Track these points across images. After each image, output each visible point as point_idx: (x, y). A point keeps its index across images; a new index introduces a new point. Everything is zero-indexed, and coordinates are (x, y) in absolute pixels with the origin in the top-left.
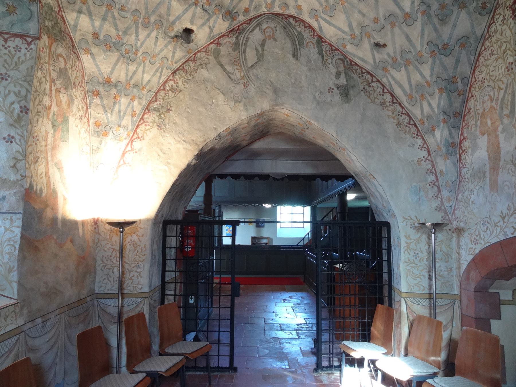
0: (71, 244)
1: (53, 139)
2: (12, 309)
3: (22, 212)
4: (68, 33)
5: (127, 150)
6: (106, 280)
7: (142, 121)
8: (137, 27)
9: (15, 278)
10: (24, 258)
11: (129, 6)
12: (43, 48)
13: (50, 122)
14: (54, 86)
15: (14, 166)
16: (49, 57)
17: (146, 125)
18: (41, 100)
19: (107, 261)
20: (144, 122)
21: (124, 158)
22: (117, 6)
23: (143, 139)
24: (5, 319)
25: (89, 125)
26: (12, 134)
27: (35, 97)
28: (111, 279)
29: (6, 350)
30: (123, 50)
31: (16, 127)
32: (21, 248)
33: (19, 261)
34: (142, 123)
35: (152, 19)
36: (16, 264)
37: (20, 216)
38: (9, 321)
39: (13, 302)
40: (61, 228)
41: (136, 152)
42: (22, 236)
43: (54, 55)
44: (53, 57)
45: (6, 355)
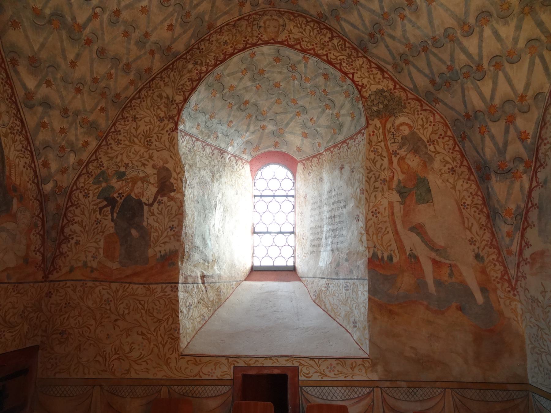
0: (460, 312)
1: (402, 206)
2: (360, 362)
3: (367, 278)
4: (413, 97)
5: (533, 186)
6: (537, 370)
7: (540, 141)
8: (460, 44)
9: (367, 336)
10: (375, 319)
11: (437, 33)
12: (373, 132)
13: (395, 192)
14: (396, 156)
15: (361, 240)
16: (384, 135)
17: (545, 145)
18: (377, 177)
19: (535, 341)
20: (543, 140)
21: (532, 199)
22: (429, 42)
23: (547, 165)
24: (351, 368)
25: (472, 173)
26: (358, 214)
27: (369, 177)
28: (541, 369)
29: (356, 396)
30: (461, 78)
31: (360, 208)
32: (370, 310)
33: (369, 321)
34: (541, 143)
35: (472, 21)
36: (366, 323)
37: (366, 282)
38: (356, 371)
39: (366, 356)
40: (435, 294)
41: (542, 186)
42: (369, 299)
43: (392, 130)
44: (389, 132)
45: (356, 400)
